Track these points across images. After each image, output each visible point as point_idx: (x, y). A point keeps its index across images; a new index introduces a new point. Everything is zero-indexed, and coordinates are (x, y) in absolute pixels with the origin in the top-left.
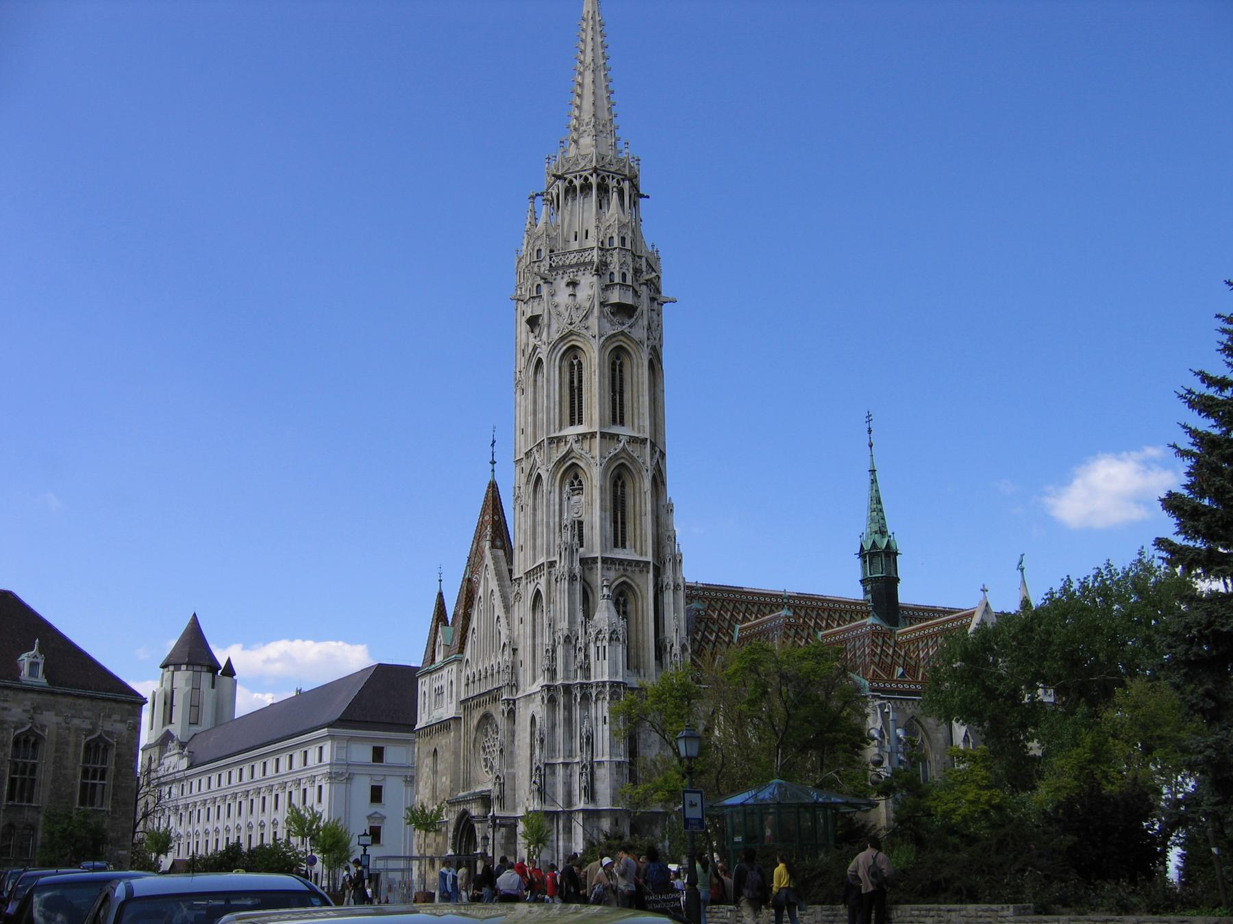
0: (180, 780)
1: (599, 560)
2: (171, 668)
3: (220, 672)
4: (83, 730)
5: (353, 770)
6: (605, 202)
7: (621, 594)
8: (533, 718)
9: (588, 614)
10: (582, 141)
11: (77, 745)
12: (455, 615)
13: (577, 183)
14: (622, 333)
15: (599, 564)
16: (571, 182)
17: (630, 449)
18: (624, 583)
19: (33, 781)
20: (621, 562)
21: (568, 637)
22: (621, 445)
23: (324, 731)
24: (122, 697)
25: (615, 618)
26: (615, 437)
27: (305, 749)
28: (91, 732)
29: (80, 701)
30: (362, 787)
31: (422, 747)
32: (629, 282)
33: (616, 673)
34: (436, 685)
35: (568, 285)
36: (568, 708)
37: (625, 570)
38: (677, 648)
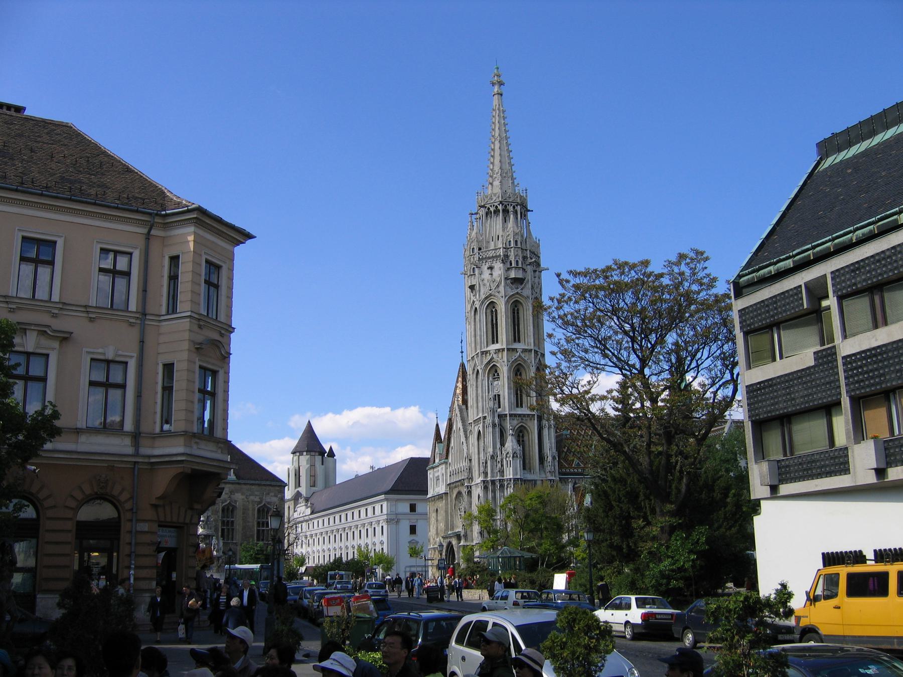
0: (307, 521)
1: (508, 415)
2: (298, 454)
3: (326, 455)
4: (256, 502)
5: (400, 517)
6: (508, 218)
7: (521, 431)
8: (479, 495)
9: (503, 444)
10: (495, 183)
11: (254, 510)
12: (445, 437)
13: (492, 209)
14: (517, 293)
15: (508, 417)
16: (489, 209)
17: (523, 355)
18: (522, 426)
19: (233, 529)
20: (520, 415)
21: (493, 456)
22: (518, 354)
23: (382, 497)
24: (273, 483)
25: (516, 446)
26: (515, 350)
27: (374, 505)
28: (260, 503)
29: (253, 487)
30: (405, 526)
31: (430, 508)
32: (520, 265)
33: (517, 474)
34: (436, 475)
35: (488, 268)
36: (494, 491)
37: (522, 419)
38: (550, 459)
